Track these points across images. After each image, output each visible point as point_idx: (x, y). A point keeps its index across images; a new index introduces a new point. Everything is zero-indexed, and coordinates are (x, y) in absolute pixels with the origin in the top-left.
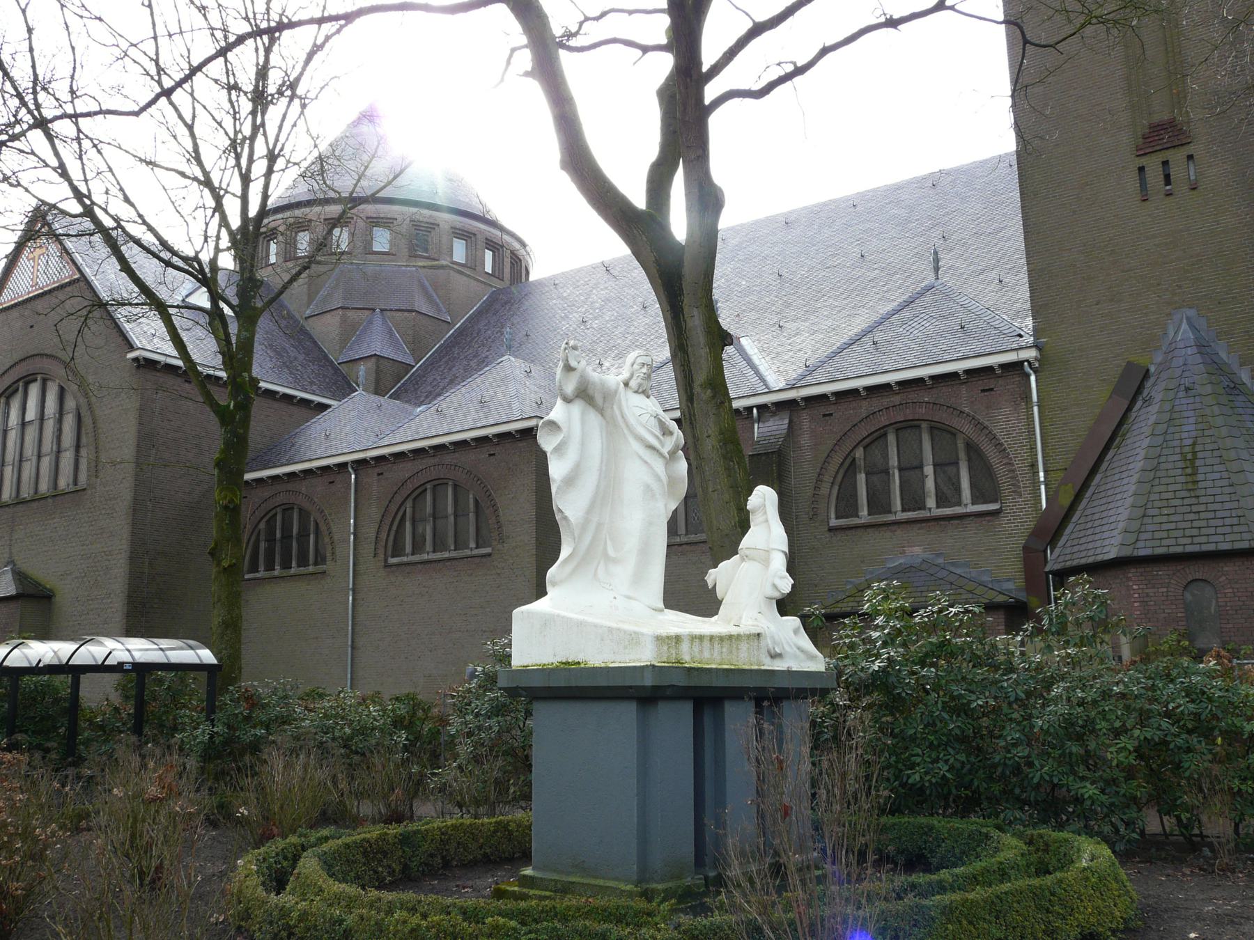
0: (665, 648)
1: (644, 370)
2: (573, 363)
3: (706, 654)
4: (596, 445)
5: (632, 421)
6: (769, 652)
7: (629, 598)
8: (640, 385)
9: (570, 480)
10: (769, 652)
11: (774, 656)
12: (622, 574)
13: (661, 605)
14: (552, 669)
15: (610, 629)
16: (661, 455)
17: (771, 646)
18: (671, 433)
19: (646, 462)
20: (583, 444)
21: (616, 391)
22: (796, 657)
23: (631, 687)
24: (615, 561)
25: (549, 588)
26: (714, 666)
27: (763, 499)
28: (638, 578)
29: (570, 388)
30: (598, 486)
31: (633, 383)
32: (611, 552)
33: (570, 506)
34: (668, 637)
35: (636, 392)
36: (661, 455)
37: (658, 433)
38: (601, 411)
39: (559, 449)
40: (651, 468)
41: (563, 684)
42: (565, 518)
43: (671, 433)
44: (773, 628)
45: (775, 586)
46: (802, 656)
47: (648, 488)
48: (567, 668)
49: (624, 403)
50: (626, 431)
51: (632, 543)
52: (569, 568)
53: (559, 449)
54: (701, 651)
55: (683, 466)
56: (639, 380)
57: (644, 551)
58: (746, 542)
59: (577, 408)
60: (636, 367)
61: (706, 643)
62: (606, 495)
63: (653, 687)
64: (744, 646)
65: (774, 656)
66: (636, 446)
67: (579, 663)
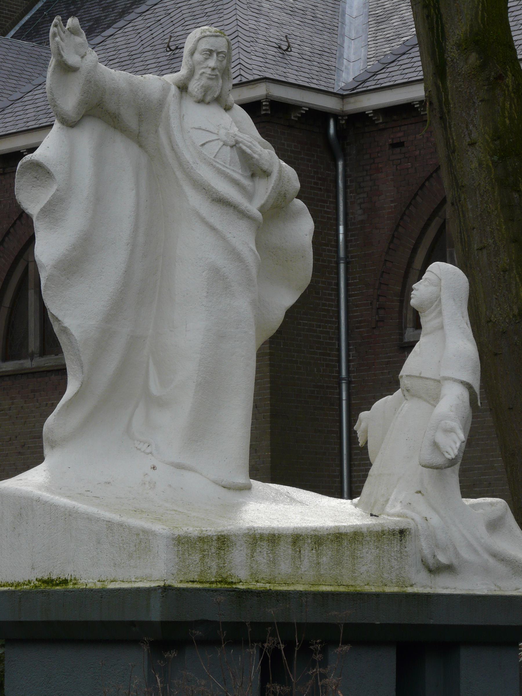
0: (196, 557)
1: (212, 63)
2: (72, 59)
3: (285, 567)
4: (125, 202)
5: (188, 155)
6: (424, 562)
7: (180, 467)
8: (206, 90)
9: (74, 264)
10: (424, 562)
11: (436, 569)
12: (171, 425)
13: (242, 477)
14: (26, 593)
15: (110, 524)
16: (243, 214)
17: (427, 552)
18: (266, 174)
19: (213, 229)
20: (99, 200)
21: (161, 103)
22: (486, 570)
23: (133, 623)
24: (160, 403)
25: (47, 451)
26: (300, 588)
27: (441, 288)
28: (200, 431)
29: (70, 102)
30: (128, 272)
31: (194, 86)
32: (155, 389)
33: (75, 310)
34: (203, 539)
35: (201, 101)
36: (243, 214)
37: (238, 174)
38: (137, 138)
39: (50, 210)
40: (222, 238)
41: (38, 617)
42: (65, 330)
43: (266, 174)
44: (435, 520)
45: (435, 445)
46: (501, 568)
47: (216, 275)
48: (52, 591)
49: (174, 123)
50: (179, 174)
51: (187, 370)
52: (76, 418)
53: (50, 210)
54: (274, 562)
55: (302, 227)
56: (204, 81)
57: (210, 385)
58: (413, 364)
59: (86, 138)
60: (198, 57)
61: (285, 550)
62: (143, 287)
63: (164, 624)
64: (368, 553)
65: (436, 569)
66: (195, 200)
67: (65, 582)
